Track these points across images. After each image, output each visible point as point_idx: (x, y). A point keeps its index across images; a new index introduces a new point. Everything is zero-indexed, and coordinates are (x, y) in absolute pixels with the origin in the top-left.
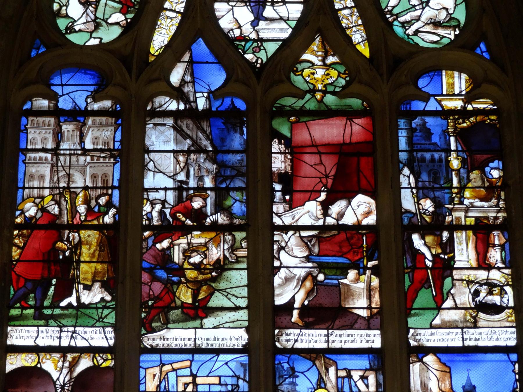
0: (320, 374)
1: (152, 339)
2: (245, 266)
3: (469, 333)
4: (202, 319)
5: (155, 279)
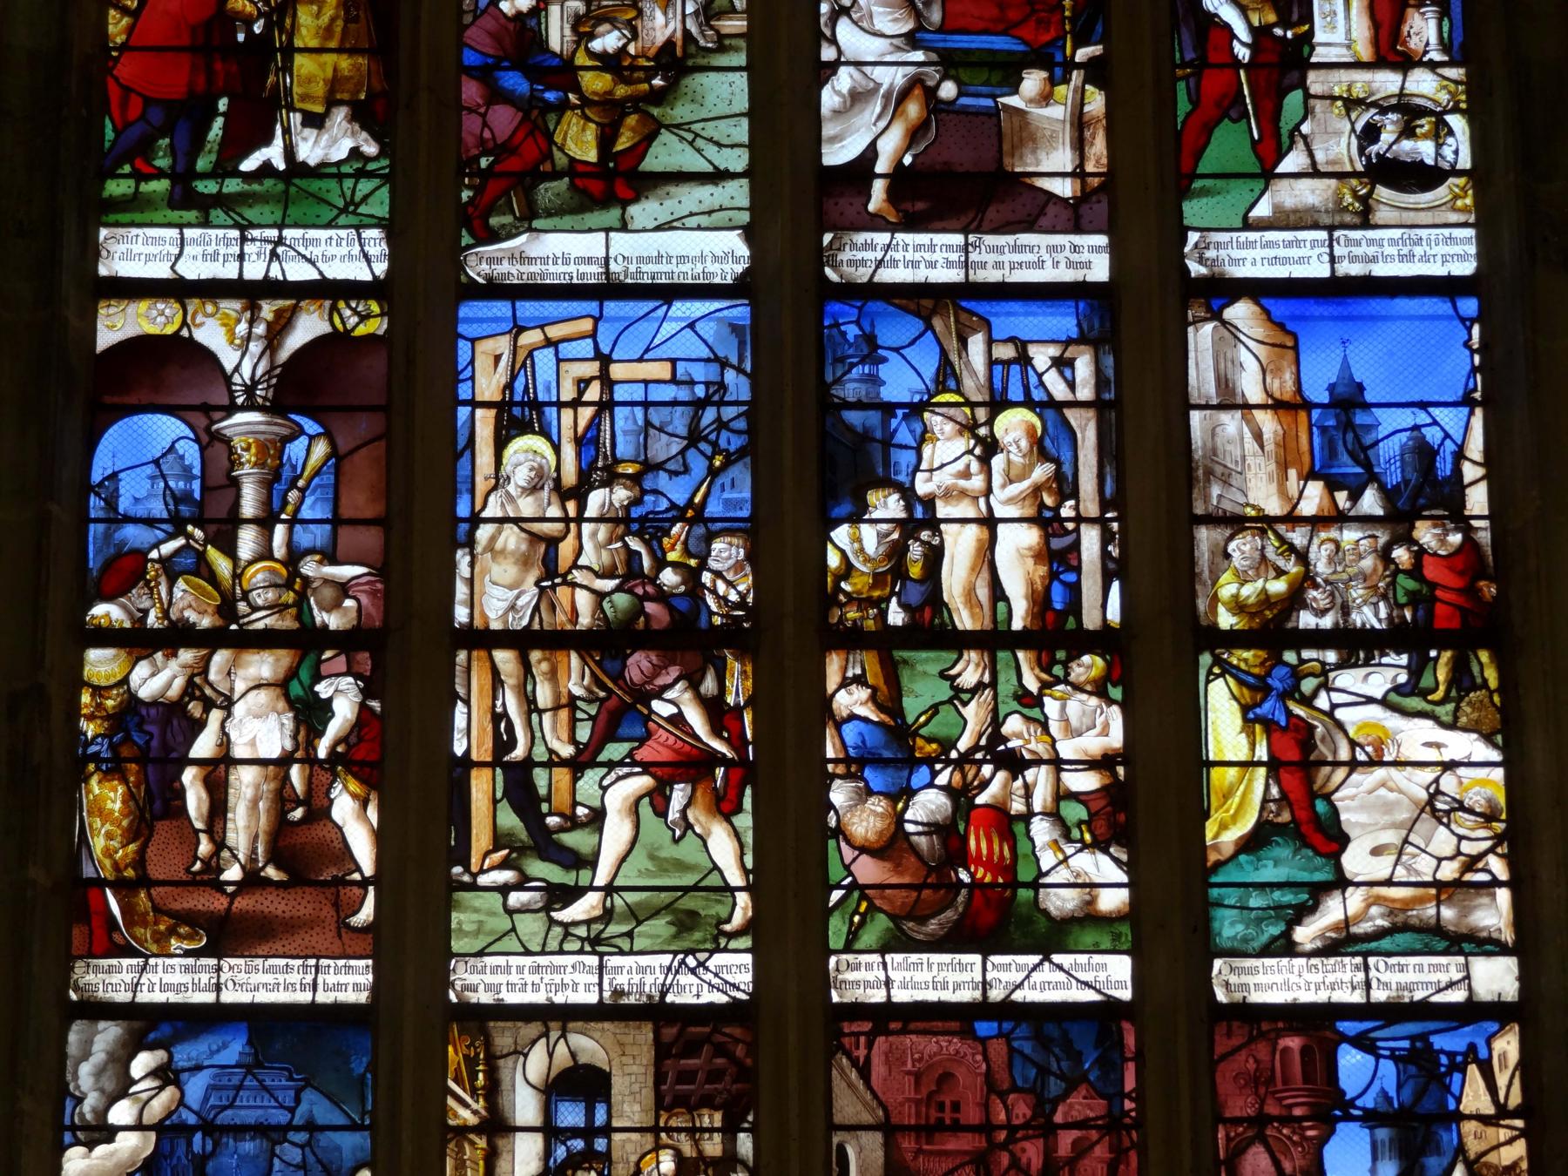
0: (944, 353)
1: (490, 261)
2: (740, 59)
3: (1349, 242)
4: (624, 204)
5: (496, 95)
